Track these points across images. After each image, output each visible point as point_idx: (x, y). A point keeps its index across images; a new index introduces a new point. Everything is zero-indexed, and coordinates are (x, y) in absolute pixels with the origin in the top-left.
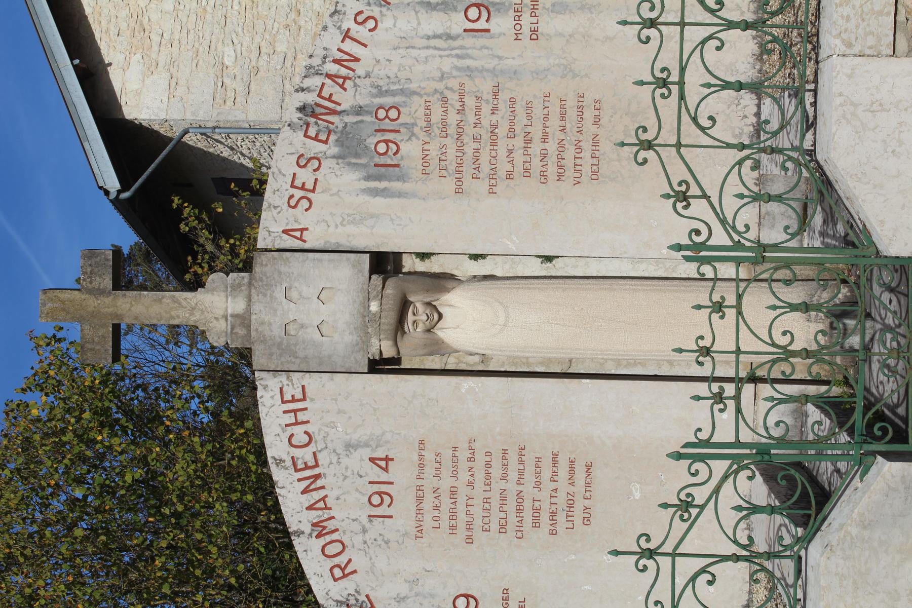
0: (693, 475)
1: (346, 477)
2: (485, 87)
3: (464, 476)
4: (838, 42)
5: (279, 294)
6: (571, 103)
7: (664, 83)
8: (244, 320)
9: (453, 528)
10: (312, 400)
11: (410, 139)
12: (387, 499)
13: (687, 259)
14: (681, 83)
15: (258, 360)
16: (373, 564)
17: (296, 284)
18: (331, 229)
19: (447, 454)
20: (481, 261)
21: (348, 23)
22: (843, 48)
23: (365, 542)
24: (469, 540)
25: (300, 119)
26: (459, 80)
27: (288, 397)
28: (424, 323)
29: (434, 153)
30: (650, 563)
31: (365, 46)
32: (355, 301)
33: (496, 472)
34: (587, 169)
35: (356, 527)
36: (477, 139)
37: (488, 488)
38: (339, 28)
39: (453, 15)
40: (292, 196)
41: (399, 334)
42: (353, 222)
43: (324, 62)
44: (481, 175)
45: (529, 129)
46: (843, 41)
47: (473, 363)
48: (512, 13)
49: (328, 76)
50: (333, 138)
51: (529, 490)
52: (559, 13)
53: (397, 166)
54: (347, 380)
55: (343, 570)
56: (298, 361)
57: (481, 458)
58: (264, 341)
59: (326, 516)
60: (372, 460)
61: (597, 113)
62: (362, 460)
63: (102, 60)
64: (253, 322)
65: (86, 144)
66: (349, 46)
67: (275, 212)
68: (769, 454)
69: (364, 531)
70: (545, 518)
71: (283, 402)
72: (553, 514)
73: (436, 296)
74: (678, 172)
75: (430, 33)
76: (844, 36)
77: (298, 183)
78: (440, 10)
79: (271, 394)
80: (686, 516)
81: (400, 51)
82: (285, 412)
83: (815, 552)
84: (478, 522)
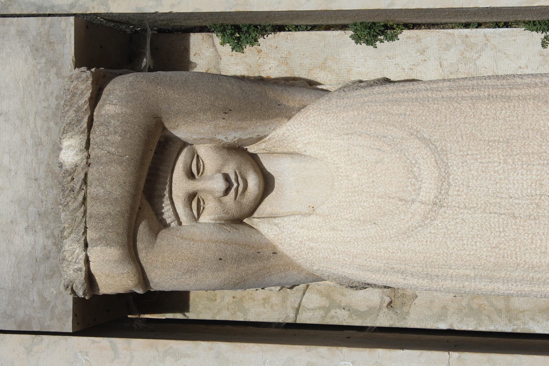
28: (219, 200)
32: (39, 144)
41: (143, 230)
54: (29, 351)
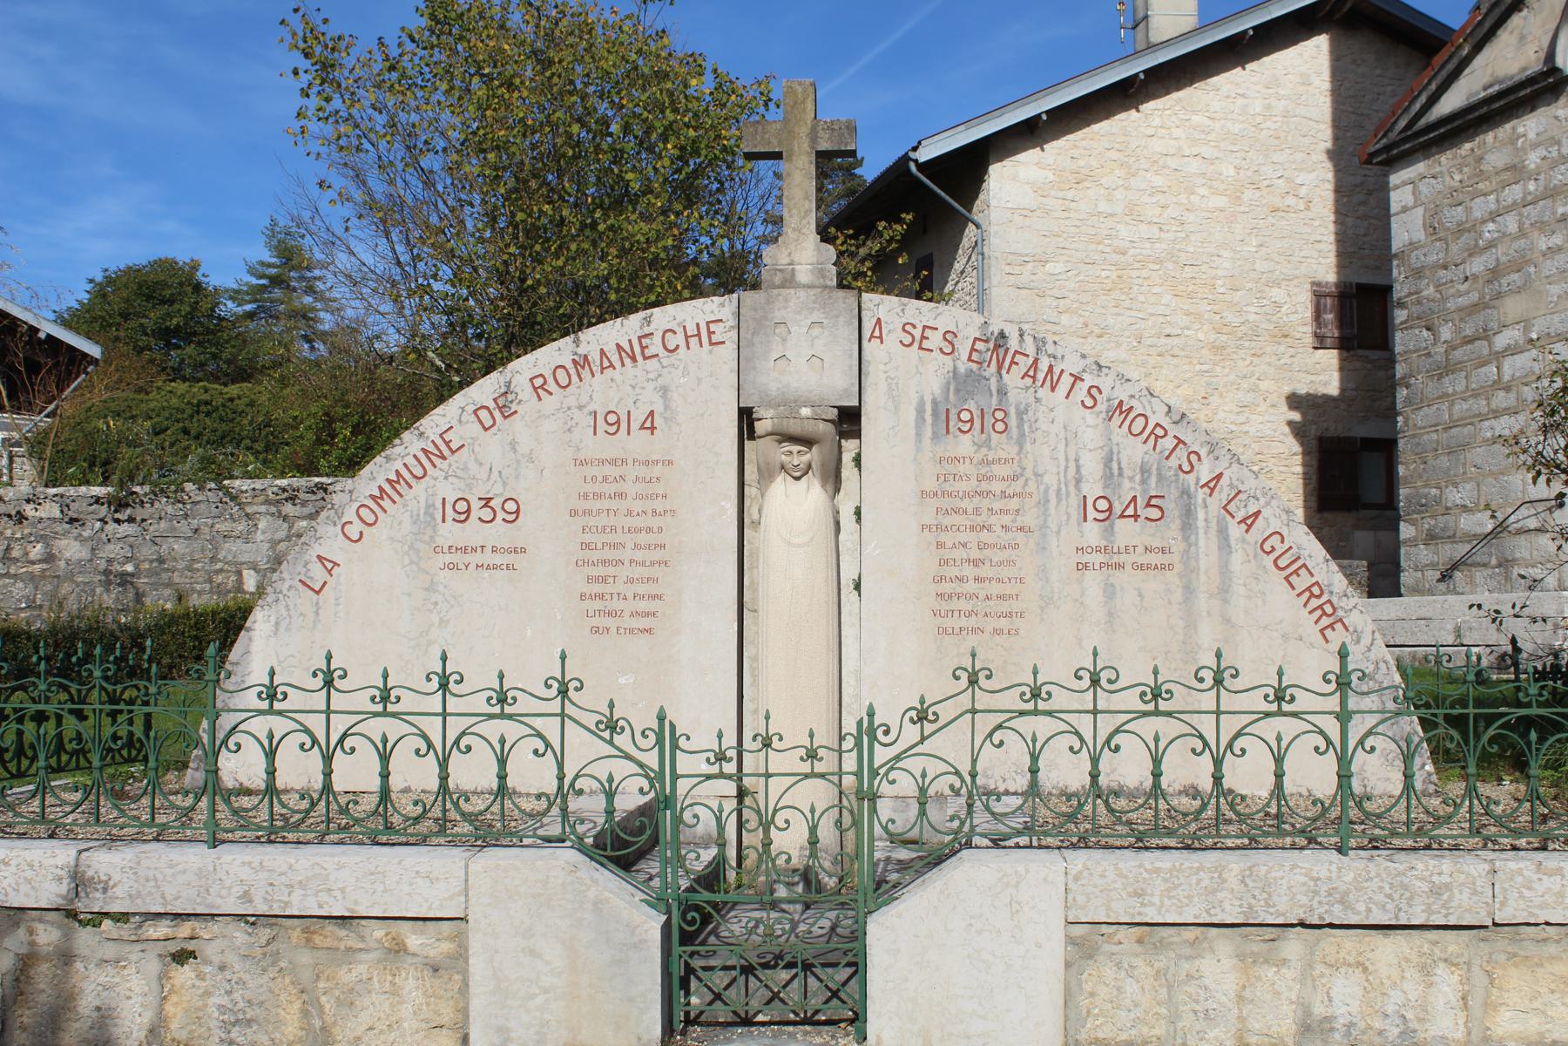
0: (643, 732)
1: (634, 387)
2: (1029, 519)
3: (637, 506)
4: (1080, 867)
5: (816, 316)
6: (1015, 606)
7: (1036, 695)
8: (789, 282)
9: (586, 496)
10: (711, 352)
11: (975, 443)
12: (613, 429)
13: (860, 723)
14: (1036, 712)
15: (749, 297)
16: (547, 417)
17: (826, 333)
18: (882, 367)
19: (659, 489)
20: (854, 518)
21: (1089, 380)
22: (1073, 872)
23: (569, 408)
24: (574, 513)
25: (992, 333)
26: (1035, 492)
27: (713, 327)
29: (962, 468)
30: (554, 692)
31: (1067, 397)
32: (811, 392)
33: (643, 538)
34: (948, 623)
35: (584, 399)
36: (977, 511)
37: (626, 530)
38: (1084, 371)
39: (1100, 485)
40: (914, 327)
42: (890, 388)
43: (1049, 356)
44: (940, 516)
45: (988, 563)
46: (1081, 872)
47: (751, 512)
48: (1104, 543)
49: (1036, 361)
50: (974, 366)
51: (625, 572)
52: (1105, 592)
53: (948, 432)
55: (541, 387)
56: (749, 336)
57: (655, 522)
58: (768, 302)
59: (594, 369)
60: (652, 413)
61: (1006, 631)
62: (652, 403)
63: (1047, 142)
64: (788, 291)
65: (962, 128)
66: (1066, 381)
67: (899, 310)
68: (666, 808)
69: (580, 408)
70: (597, 588)
71: (708, 323)
72: (601, 596)
73: (818, 474)
74: (946, 712)
75: (1081, 462)
76: (1086, 873)
77: (928, 333)
78: (1105, 472)
79: (716, 311)
80: (602, 727)
81: (1063, 432)
82: (698, 325)
83: (568, 855)
84: (592, 521)
